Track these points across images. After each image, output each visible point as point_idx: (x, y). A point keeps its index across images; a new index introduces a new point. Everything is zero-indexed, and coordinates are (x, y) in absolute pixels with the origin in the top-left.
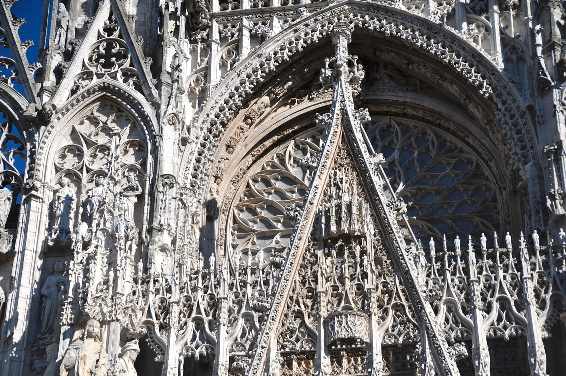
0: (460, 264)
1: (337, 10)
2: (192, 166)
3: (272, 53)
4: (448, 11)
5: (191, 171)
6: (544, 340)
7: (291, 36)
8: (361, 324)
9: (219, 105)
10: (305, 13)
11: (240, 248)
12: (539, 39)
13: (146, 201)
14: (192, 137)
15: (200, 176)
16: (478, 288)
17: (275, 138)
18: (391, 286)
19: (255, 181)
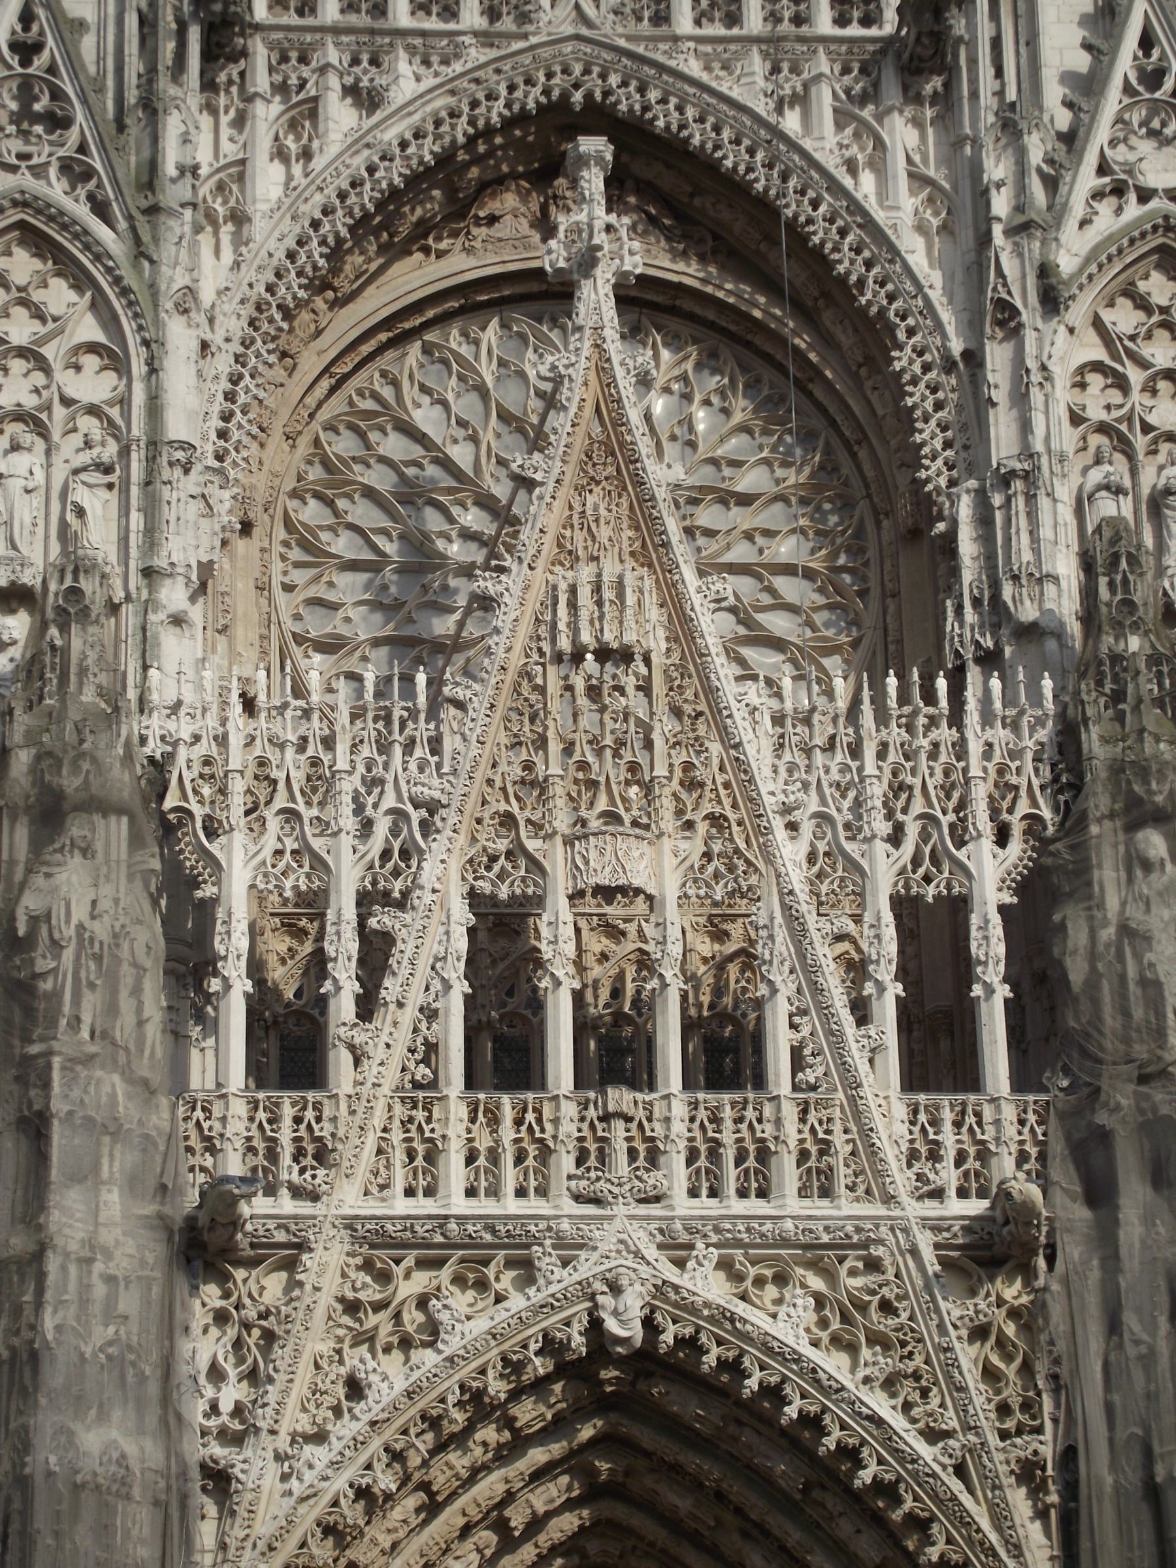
0: (846, 735)
1: (545, 53)
2: (216, 409)
3: (395, 143)
4: (794, 88)
5: (216, 423)
6: (1002, 909)
7: (442, 102)
8: (642, 855)
9: (275, 262)
10: (473, 51)
11: (300, 596)
12: (1001, 204)
13: (134, 502)
14: (217, 338)
15: (236, 435)
16: (877, 791)
17: (383, 337)
18: (700, 773)
19: (331, 427)
